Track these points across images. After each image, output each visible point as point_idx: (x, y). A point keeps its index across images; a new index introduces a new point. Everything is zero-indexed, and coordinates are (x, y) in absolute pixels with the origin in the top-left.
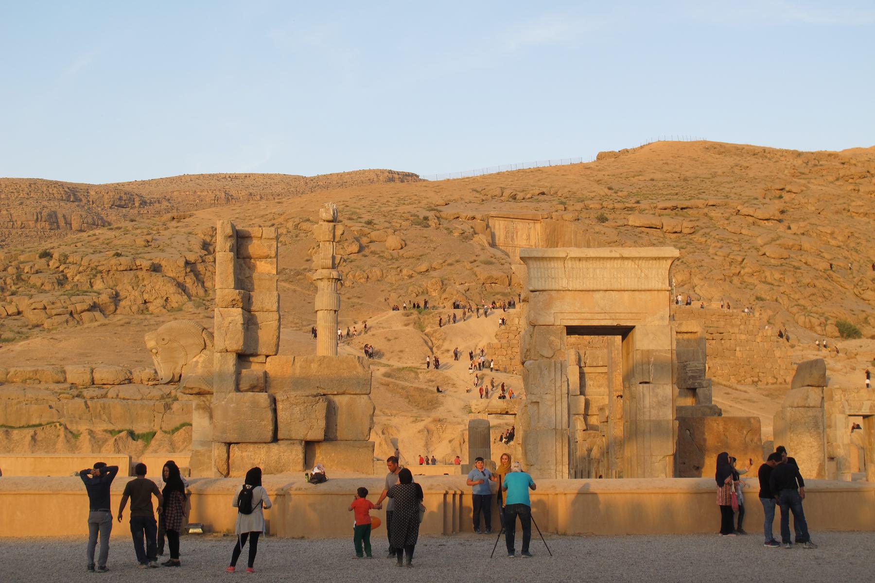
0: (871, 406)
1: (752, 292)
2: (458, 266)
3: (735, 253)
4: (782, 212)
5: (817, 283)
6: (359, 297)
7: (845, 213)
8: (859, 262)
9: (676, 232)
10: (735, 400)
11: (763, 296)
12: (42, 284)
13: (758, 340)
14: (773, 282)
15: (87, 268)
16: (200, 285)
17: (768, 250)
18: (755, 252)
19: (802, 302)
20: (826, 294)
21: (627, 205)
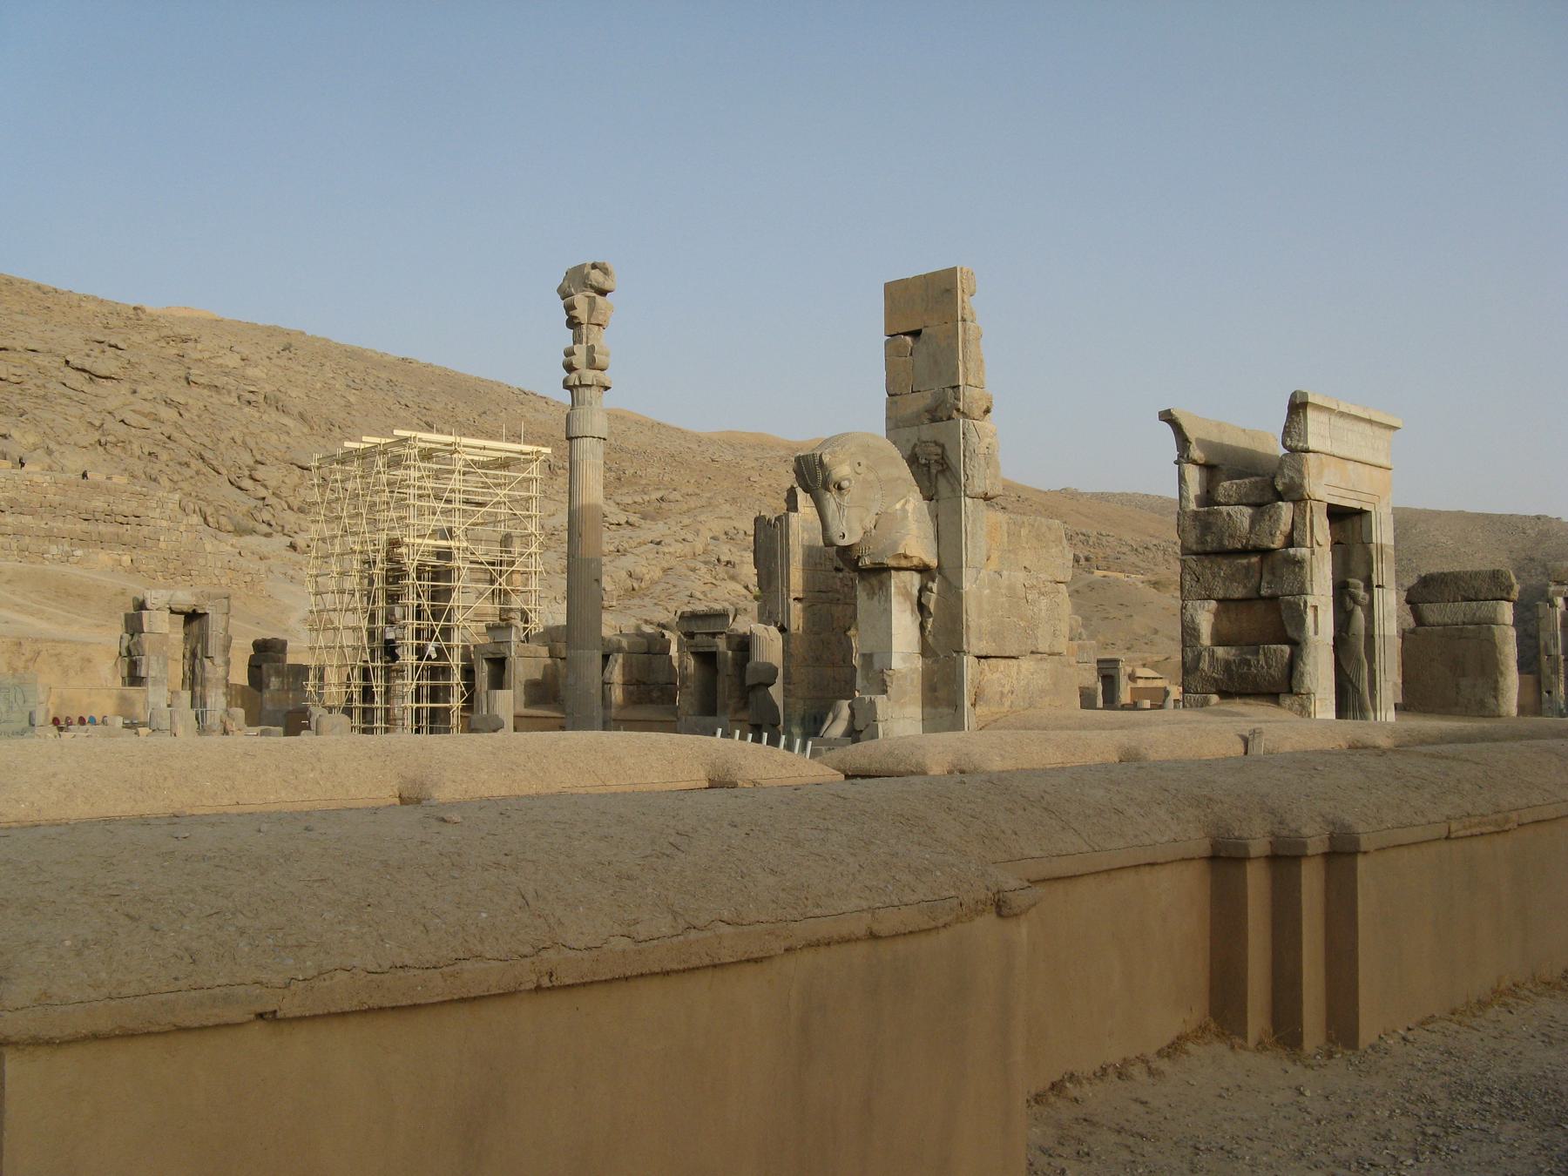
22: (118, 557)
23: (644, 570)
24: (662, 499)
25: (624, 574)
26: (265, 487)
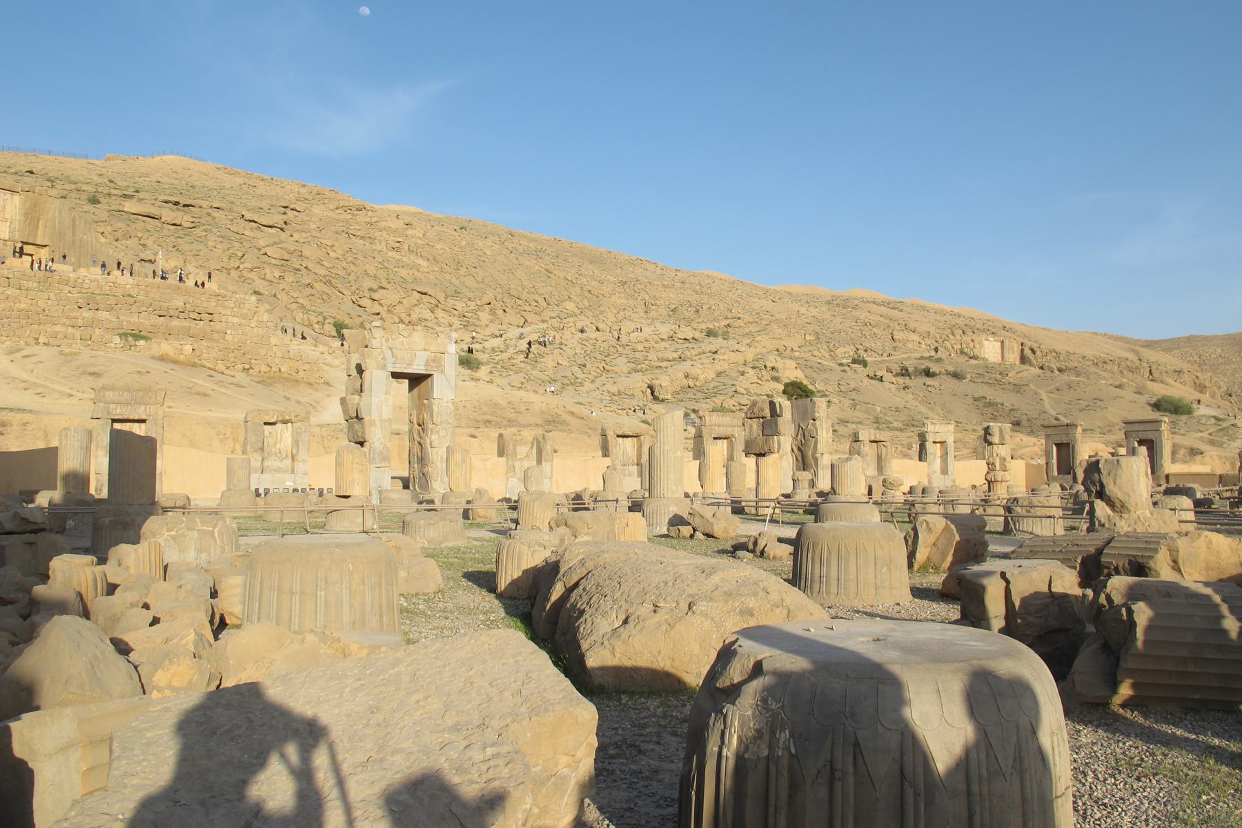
0: (428, 360)
1: (250, 286)
5: (316, 285)
8: (356, 273)
10: (219, 383)
11: (262, 291)
17: (270, 251)
18: (256, 251)
19: (300, 300)
20: (325, 297)
21: (125, 193)
22: (179, 347)
23: (699, 372)
24: (728, 325)
25: (681, 375)
26: (381, 305)
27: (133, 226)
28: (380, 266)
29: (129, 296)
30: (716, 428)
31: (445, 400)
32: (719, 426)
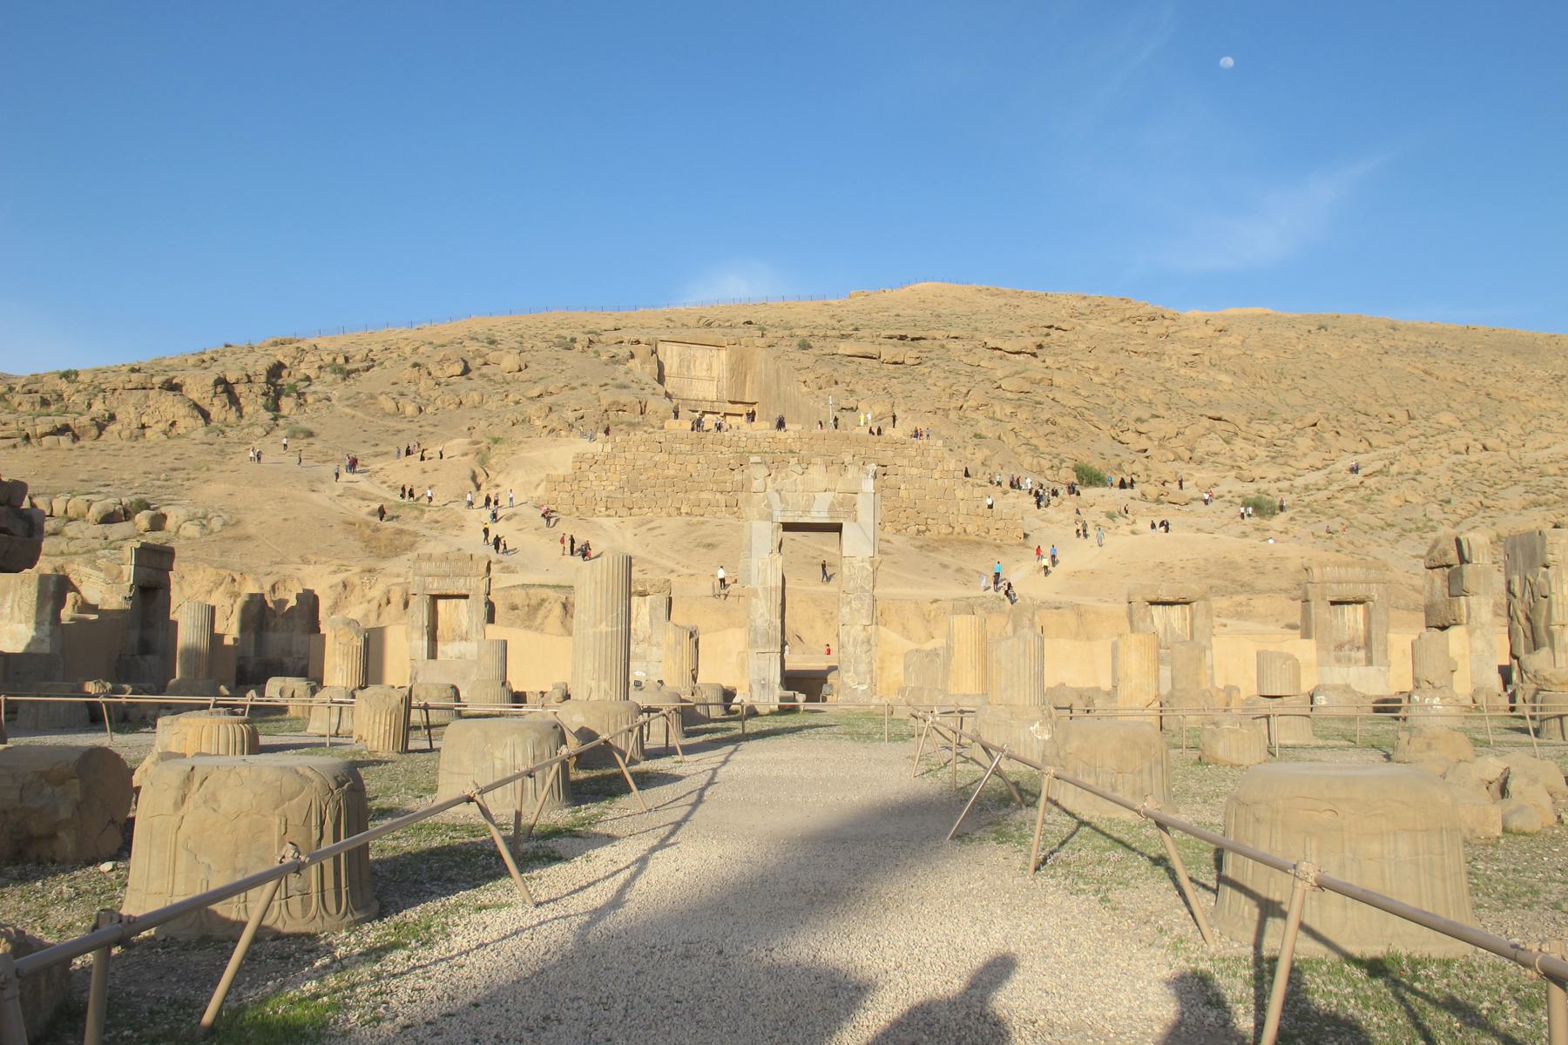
2: (582, 391)
3: (961, 384)
4: (1040, 347)
5: (1059, 420)
6: (436, 426)
7: (1123, 353)
9: (896, 363)
11: (984, 433)
12: (20, 404)
13: (936, 476)
14: (1004, 418)
15: (90, 385)
16: (234, 408)
19: (1033, 441)
20: (1071, 434)
26: (1150, 438)
27: (841, 369)
28: (1160, 388)
29: (791, 451)
30: (1334, 586)
31: (859, 558)
32: (1339, 583)
